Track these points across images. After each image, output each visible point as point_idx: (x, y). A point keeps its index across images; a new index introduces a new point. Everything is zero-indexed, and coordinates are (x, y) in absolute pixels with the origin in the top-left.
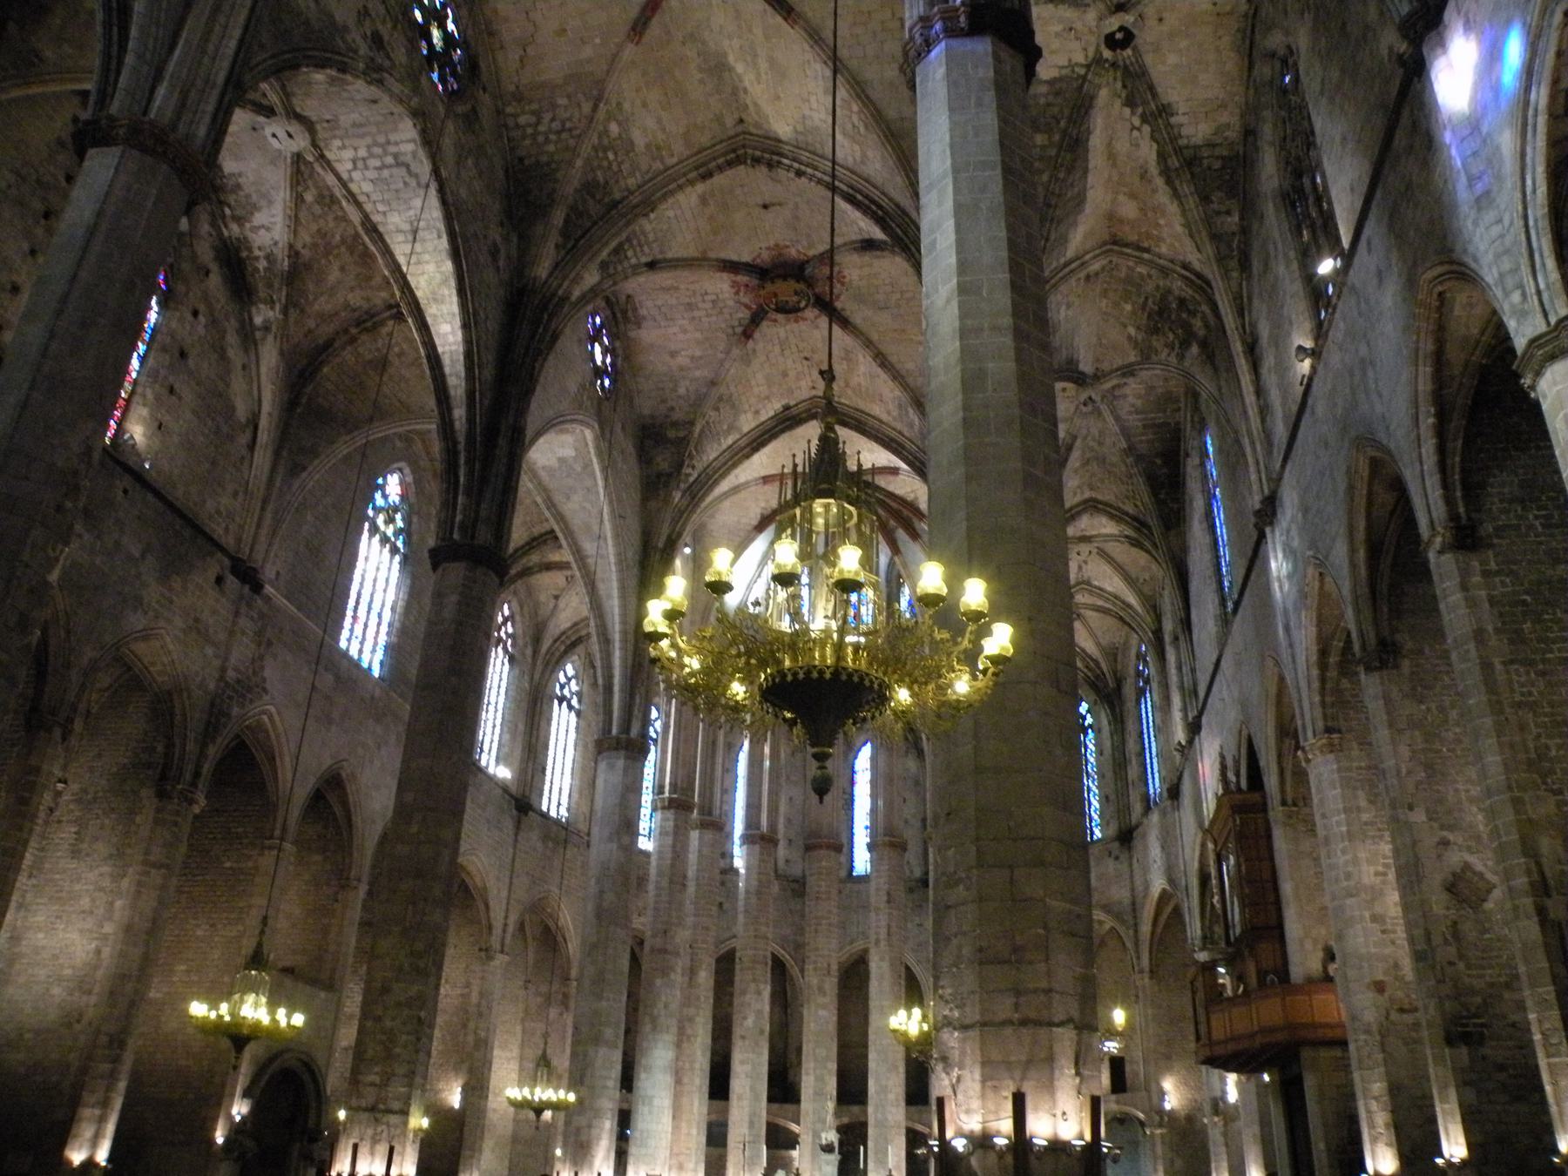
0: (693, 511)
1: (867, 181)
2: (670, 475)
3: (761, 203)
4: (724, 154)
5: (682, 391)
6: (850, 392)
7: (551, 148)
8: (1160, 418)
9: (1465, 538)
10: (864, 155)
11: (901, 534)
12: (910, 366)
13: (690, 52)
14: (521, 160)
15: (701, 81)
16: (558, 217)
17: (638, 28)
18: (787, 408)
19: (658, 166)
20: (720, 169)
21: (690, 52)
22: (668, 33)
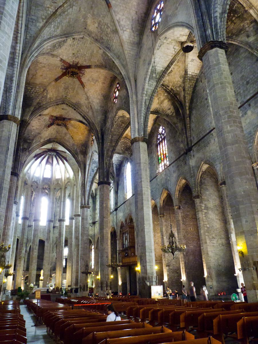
0: (29, 156)
1: (88, 115)
2: (26, 149)
3: (62, 108)
4: (61, 101)
5: (32, 133)
6: (63, 139)
7: (33, 95)
8: (120, 159)
9: (179, 208)
10: (89, 111)
11: (60, 162)
12: (77, 139)
13: (63, 85)
14: (26, 95)
15: (63, 90)
16: (32, 109)
17: (56, 80)
18: (50, 139)
19: (50, 101)
20: (60, 104)
21: (63, 85)
22: (61, 82)
